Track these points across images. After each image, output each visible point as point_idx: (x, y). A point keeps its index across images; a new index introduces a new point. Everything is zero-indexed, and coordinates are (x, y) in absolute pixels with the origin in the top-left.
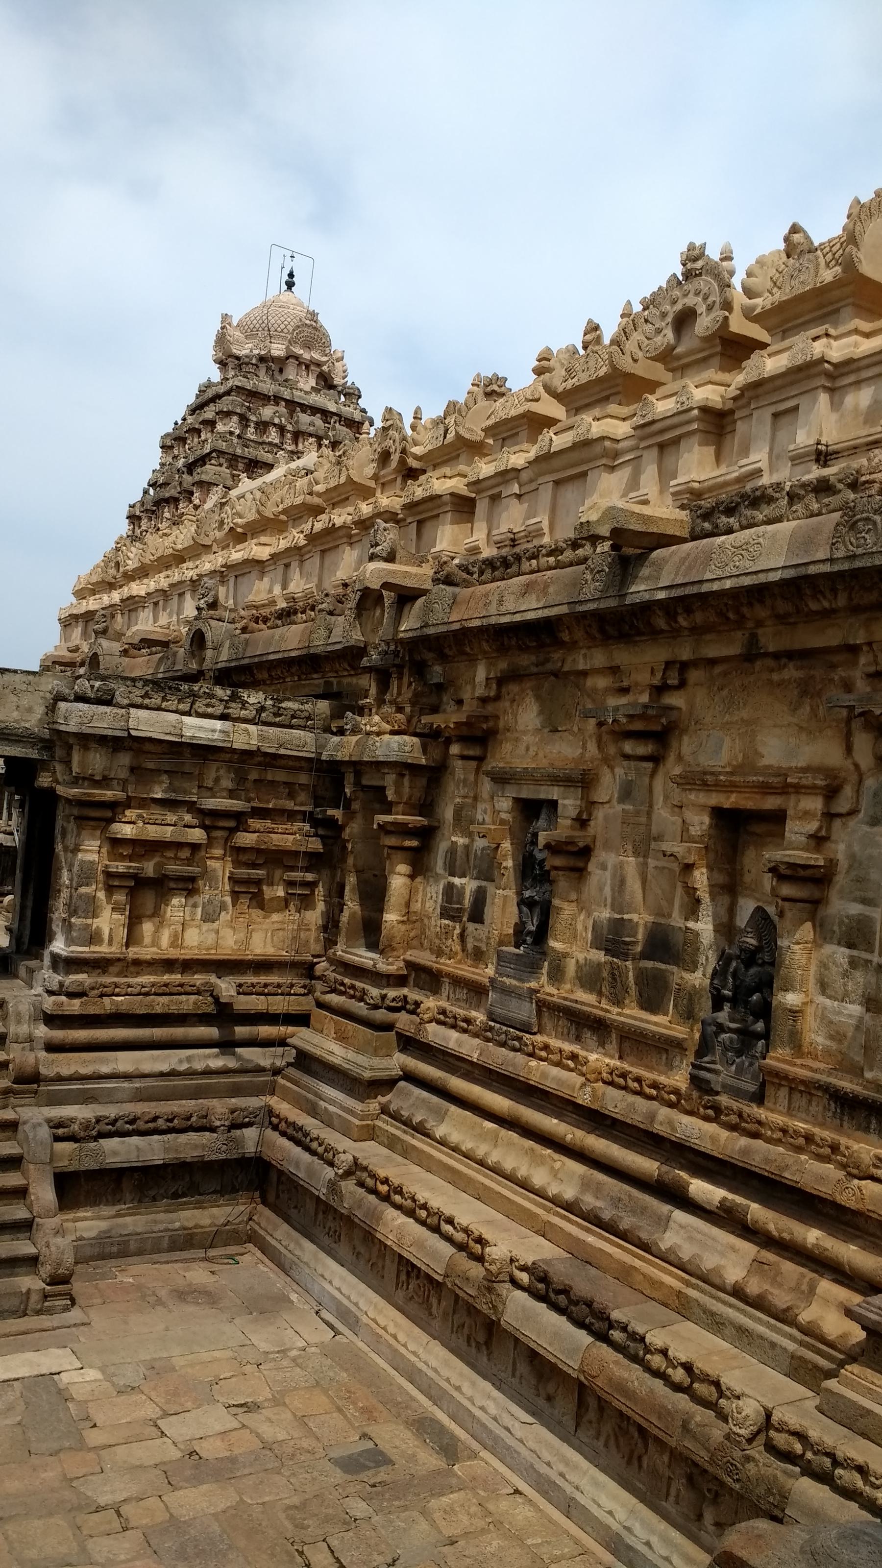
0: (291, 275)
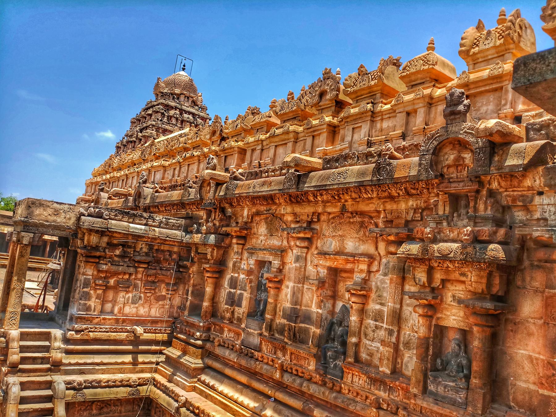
0: (184, 66)
